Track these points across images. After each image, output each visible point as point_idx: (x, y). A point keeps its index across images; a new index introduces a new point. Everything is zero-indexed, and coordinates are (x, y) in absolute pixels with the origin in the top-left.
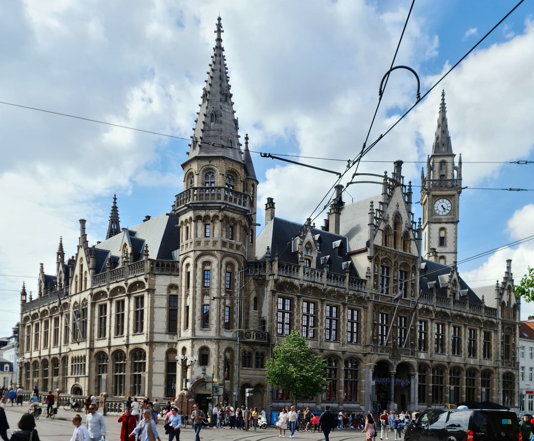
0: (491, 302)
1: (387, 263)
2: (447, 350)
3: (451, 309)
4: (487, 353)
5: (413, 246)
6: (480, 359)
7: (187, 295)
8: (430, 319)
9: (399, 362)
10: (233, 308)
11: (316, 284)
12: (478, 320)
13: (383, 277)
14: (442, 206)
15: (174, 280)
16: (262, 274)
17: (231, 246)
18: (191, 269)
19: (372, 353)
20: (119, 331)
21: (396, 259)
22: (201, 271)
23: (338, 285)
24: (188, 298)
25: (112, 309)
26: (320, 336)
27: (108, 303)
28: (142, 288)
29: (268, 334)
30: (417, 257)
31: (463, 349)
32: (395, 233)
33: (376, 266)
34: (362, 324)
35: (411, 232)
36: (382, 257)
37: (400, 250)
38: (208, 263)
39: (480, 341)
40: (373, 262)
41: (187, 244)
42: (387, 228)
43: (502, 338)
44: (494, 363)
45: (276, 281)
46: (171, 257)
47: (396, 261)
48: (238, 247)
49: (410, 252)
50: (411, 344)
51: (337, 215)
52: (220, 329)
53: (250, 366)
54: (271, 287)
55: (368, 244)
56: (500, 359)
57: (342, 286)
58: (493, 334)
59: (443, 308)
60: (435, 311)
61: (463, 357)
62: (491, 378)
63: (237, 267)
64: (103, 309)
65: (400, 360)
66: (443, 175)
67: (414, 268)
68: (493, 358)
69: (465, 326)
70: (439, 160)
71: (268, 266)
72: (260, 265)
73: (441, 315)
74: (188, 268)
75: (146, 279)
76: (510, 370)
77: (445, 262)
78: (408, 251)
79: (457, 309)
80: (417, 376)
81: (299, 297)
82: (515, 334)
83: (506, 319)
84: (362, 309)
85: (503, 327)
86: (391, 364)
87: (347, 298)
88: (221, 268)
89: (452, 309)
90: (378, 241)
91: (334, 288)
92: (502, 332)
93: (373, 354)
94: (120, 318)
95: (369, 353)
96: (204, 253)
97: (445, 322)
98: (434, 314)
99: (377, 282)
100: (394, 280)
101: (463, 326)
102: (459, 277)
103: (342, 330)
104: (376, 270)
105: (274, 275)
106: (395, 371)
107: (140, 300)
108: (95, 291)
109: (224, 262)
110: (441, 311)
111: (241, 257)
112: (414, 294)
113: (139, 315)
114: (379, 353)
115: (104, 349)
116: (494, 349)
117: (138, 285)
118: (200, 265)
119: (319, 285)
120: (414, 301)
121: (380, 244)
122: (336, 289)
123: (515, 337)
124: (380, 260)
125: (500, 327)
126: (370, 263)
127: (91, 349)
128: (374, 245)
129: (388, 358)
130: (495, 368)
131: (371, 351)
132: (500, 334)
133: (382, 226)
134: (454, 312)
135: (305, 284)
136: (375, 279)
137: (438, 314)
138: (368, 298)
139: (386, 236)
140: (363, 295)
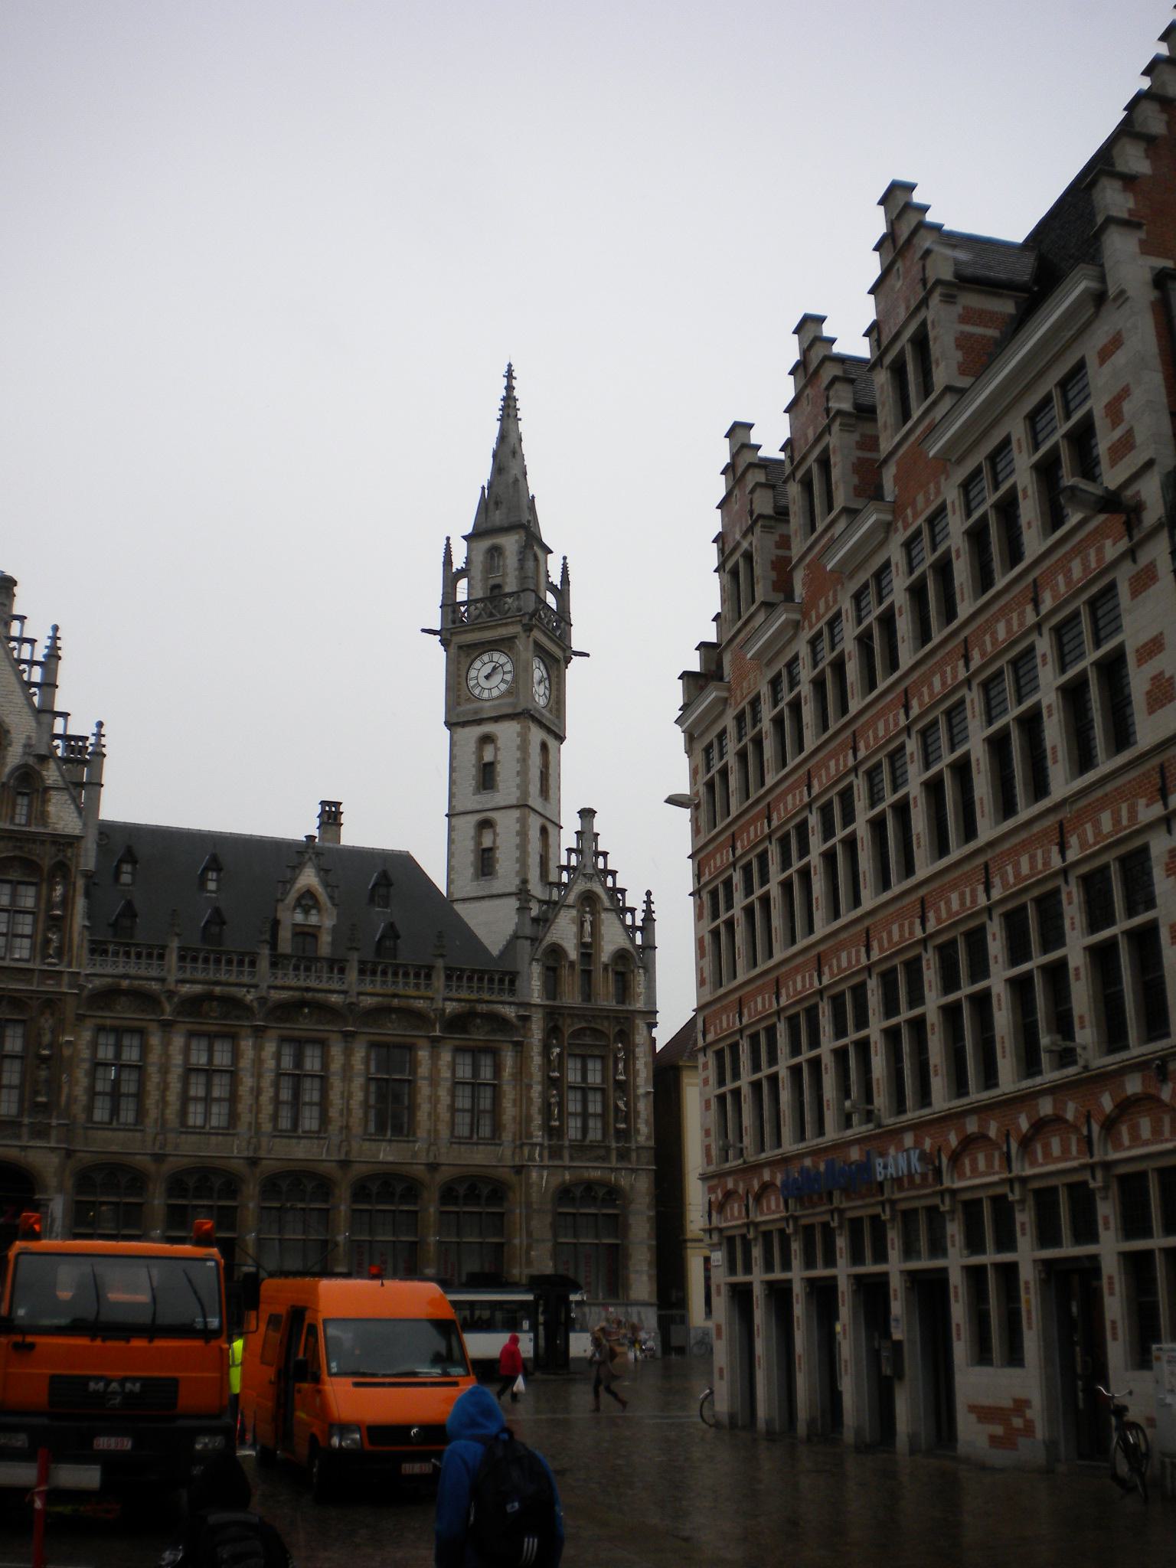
2: (246, 1118)
30: (78, 838)
31: (333, 1113)
44: (514, 1154)
49: (45, 824)
56: (538, 1136)
60: (171, 994)
66: (497, 587)
67: (62, 870)
68: (507, 1136)
69: (348, 1036)
76: (596, 1174)
98: (168, 1008)
116: (515, 1105)
125: (536, 1032)
130: (519, 1170)
137: (193, 1006)
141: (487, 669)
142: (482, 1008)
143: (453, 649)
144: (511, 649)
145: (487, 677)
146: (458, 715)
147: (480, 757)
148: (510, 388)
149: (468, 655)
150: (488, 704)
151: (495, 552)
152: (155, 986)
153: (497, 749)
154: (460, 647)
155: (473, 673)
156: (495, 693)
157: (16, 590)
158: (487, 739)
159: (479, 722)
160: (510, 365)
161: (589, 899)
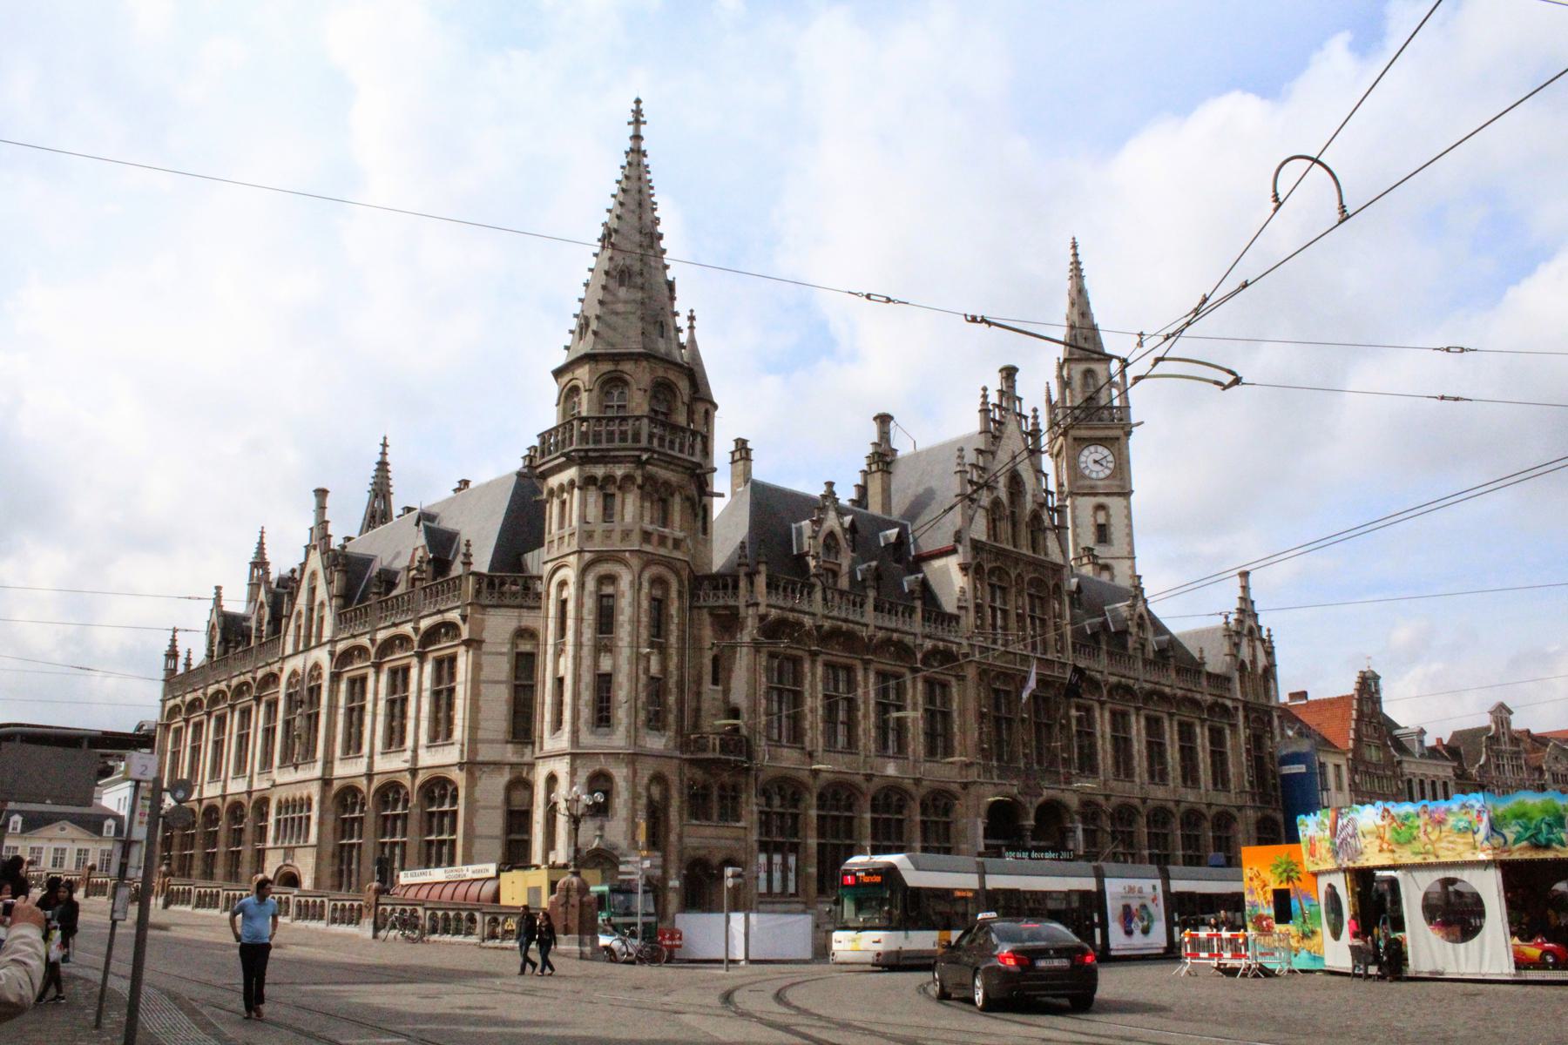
0: (1216, 661)
1: (1000, 579)
2: (1137, 770)
3: (1142, 677)
4: (1220, 777)
5: (1051, 542)
6: (1207, 791)
7: (559, 652)
8: (1099, 701)
9: (1041, 800)
10: (666, 683)
11: (851, 625)
12: (1196, 704)
13: (994, 609)
14: (1096, 462)
15: (529, 620)
16: (731, 602)
17: (663, 540)
18: (570, 592)
19: (982, 780)
20: (395, 737)
21: (1019, 571)
22: (594, 596)
23: (900, 626)
24: (562, 660)
25: (378, 687)
26: (865, 744)
27: (371, 673)
28: (453, 639)
29: (748, 741)
30: (1062, 567)
32: (1013, 513)
33: (978, 585)
34: (955, 715)
35: (1045, 511)
36: (990, 565)
37: (1026, 551)
38: (611, 579)
39: (1204, 748)
40: (970, 576)
41: (561, 538)
42: (996, 503)
43: (1248, 740)
45: (762, 618)
46: (519, 566)
47: (1019, 575)
48: (677, 544)
49: (1046, 554)
50: (1063, 758)
51: (885, 475)
52: (636, 729)
53: (708, 817)
54: (751, 633)
55: (958, 537)
56: (1248, 788)
57: (907, 628)
58: (1228, 732)
59: (1123, 676)
60: (1107, 683)
61: (1172, 785)
62: (1231, 833)
63: (674, 587)
64: (358, 684)
65: (1041, 795)
67: (1058, 588)
68: (1232, 787)
70: (1083, 366)
71: (743, 584)
72: (725, 582)
73: (1120, 691)
74: (562, 590)
75: (464, 618)
77: (1112, 577)
78: (1043, 553)
79: (1152, 679)
80: (1080, 834)
81: (814, 655)
82: (1272, 733)
83: (1251, 698)
84: (953, 682)
85: (1246, 717)
86: (1024, 807)
87: (919, 656)
88: (639, 590)
89: (1141, 678)
90: (979, 531)
91: (889, 633)
92: (1245, 728)
93: (982, 784)
94: (397, 708)
95: (975, 782)
96: (600, 558)
97: (1128, 708)
99: (982, 619)
100: (1018, 615)
101: (1165, 716)
102: (1149, 612)
103: (911, 728)
104: (979, 594)
105: (757, 605)
106: (1033, 823)
107: (446, 665)
108: (340, 647)
109: (646, 575)
110: (1120, 682)
111: (685, 565)
112: (1062, 648)
113: (443, 698)
114: (996, 781)
115: (356, 779)
117: (443, 630)
118: (591, 585)
119: (857, 627)
120: (1062, 660)
121: (984, 538)
122: (895, 636)
123: (1272, 738)
124: (986, 571)
126: (966, 578)
127: (326, 782)
128: (971, 539)
129: (1015, 790)
130: (1240, 808)
131: (979, 776)
132: (1243, 733)
133: (985, 498)
134: (1147, 686)
135: (827, 624)
136: (977, 612)
138: (966, 655)
139: (994, 520)
140: (954, 648)
141: (1098, 457)
142: (1220, 700)
143: (1070, 440)
144: (1112, 445)
145: (1096, 462)
146: (1079, 488)
147: (1096, 520)
148: (1076, 255)
149: (1079, 445)
150: (1099, 483)
151: (1089, 373)
152: (1098, 676)
153: (1108, 516)
154: (1075, 439)
155: (1083, 459)
156: (1102, 475)
157: (1018, 377)
158: (1100, 507)
159: (1095, 495)
160: (1074, 239)
161: (1251, 631)
